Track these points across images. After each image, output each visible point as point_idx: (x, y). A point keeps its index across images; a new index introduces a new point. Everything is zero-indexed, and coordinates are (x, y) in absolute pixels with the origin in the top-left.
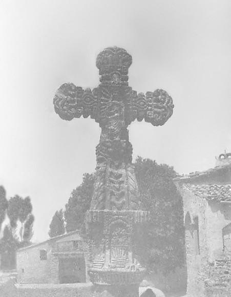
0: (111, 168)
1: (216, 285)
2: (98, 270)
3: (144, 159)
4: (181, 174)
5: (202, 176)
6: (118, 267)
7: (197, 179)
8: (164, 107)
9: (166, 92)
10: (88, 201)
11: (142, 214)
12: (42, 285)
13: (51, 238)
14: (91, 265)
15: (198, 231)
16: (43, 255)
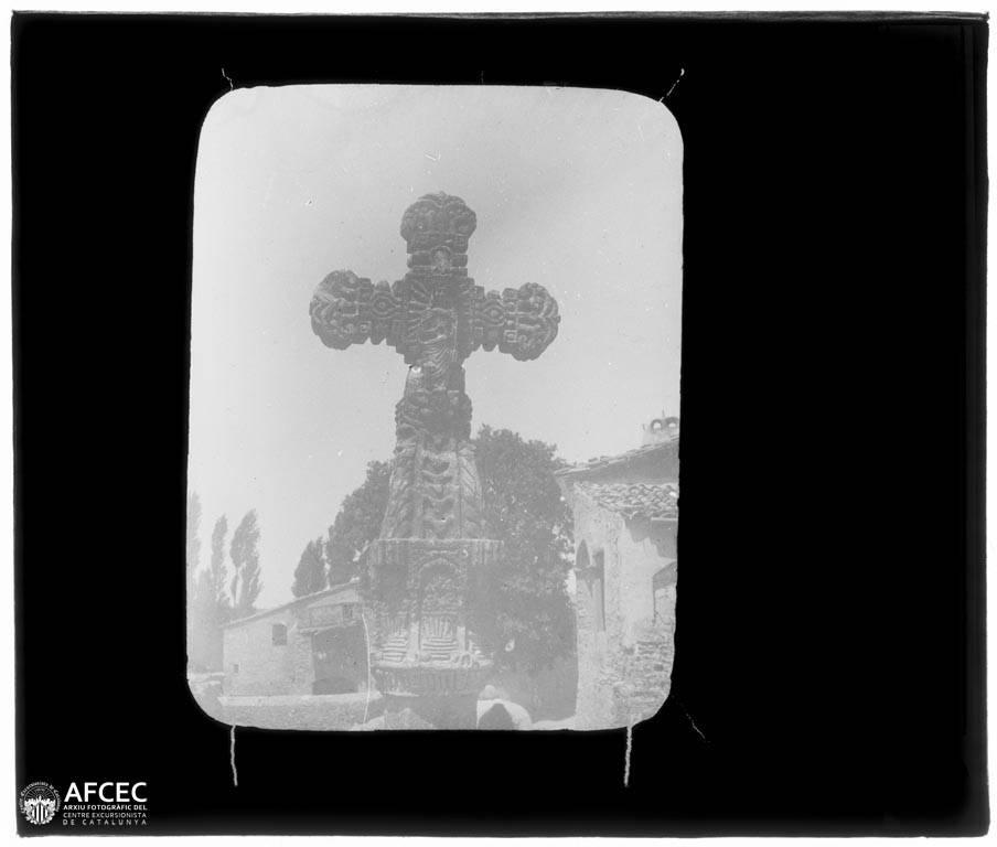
0: (425, 448)
1: (637, 694)
2: (394, 665)
3: (495, 430)
4: (570, 462)
5: (614, 465)
6: (436, 659)
7: (603, 471)
8: (538, 321)
9: (544, 289)
10: (377, 521)
11: (487, 547)
12: (275, 697)
13: (297, 599)
14: (379, 654)
15: (603, 581)
16: (279, 635)
